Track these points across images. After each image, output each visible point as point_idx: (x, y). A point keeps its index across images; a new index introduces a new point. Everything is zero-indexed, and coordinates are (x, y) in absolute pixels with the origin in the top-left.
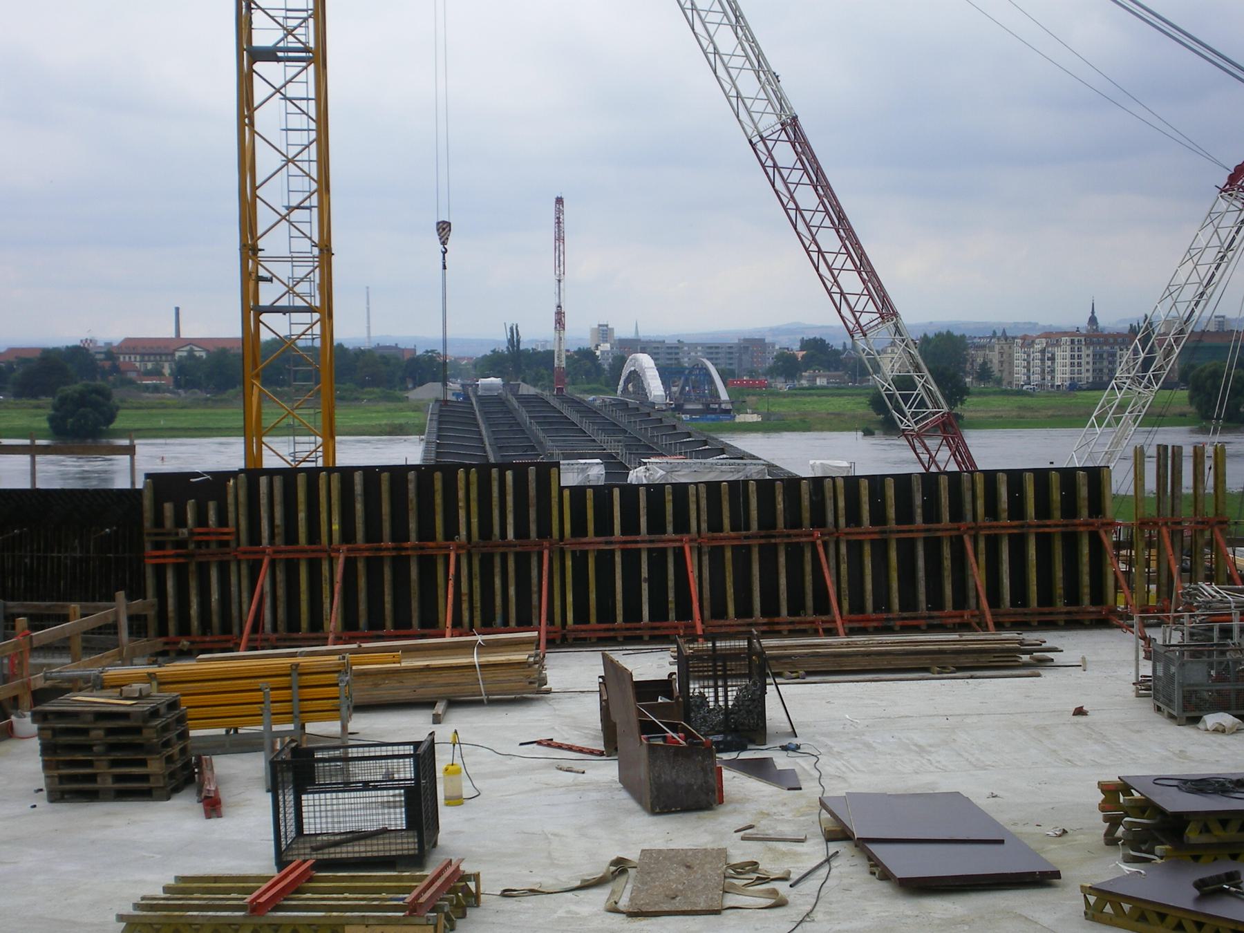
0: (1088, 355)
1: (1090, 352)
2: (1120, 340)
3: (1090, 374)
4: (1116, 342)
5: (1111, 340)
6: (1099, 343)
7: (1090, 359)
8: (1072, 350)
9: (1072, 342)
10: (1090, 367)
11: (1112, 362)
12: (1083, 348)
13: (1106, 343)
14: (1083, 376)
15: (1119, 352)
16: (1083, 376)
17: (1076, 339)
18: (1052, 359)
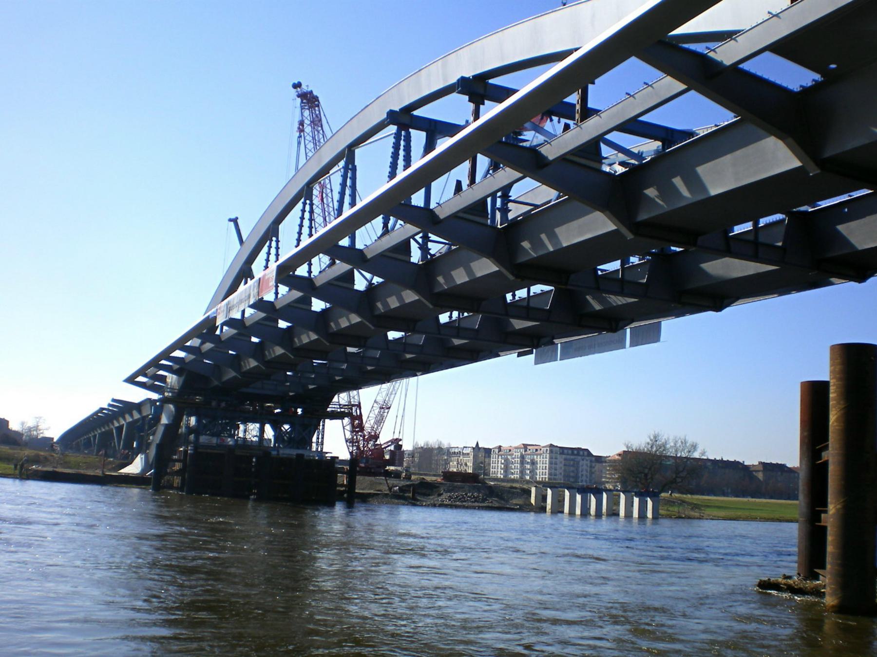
0: (561, 462)
1: (562, 460)
2: (581, 453)
3: (561, 477)
4: (578, 454)
5: (575, 452)
6: (568, 454)
7: (562, 465)
8: (551, 458)
9: (551, 451)
10: (561, 471)
11: (577, 469)
12: (558, 456)
13: (573, 454)
14: (557, 477)
15: (581, 463)
16: (557, 477)
17: (554, 449)
18: (533, 463)
